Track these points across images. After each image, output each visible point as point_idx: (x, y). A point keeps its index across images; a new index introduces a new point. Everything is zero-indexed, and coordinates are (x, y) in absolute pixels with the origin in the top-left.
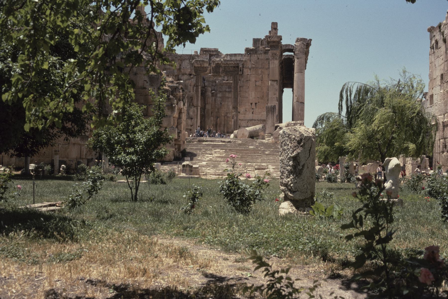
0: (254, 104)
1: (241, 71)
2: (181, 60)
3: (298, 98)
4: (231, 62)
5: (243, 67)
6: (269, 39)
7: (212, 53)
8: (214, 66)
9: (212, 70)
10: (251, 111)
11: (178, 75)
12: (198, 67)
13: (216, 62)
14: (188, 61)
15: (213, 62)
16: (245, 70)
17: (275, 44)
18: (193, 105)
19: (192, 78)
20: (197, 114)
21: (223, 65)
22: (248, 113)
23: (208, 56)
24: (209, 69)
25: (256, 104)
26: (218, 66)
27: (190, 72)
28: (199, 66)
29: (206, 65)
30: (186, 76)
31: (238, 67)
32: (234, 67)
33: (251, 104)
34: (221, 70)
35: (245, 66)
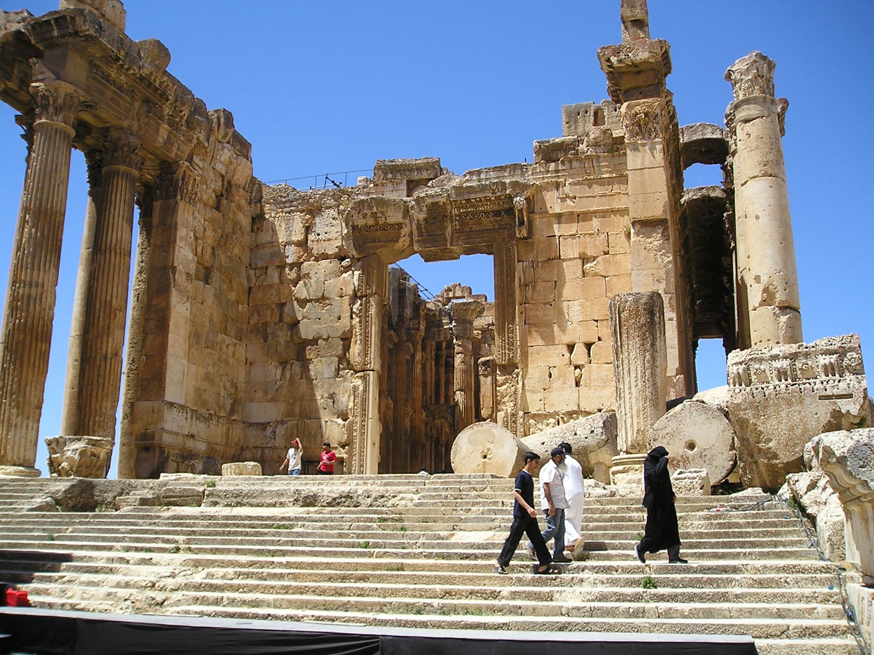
0: (580, 349)
1: (522, 223)
2: (310, 212)
3: (766, 290)
4: (480, 195)
5: (531, 211)
6: (614, 59)
7: (416, 176)
8: (422, 216)
9: (415, 233)
10: (574, 373)
11: (297, 265)
12: (367, 227)
13: (430, 201)
14: (333, 213)
15: (418, 200)
16: (538, 221)
17: (641, 80)
18: (350, 366)
19: (347, 269)
20: (364, 401)
21: (455, 212)
22: (556, 384)
23: (404, 187)
24: (405, 230)
25: (588, 346)
26: (436, 213)
27: (340, 248)
28: (371, 222)
29: (395, 217)
30: (324, 263)
31: (510, 210)
32: (497, 213)
33: (571, 348)
34: (449, 229)
35: (537, 208)
